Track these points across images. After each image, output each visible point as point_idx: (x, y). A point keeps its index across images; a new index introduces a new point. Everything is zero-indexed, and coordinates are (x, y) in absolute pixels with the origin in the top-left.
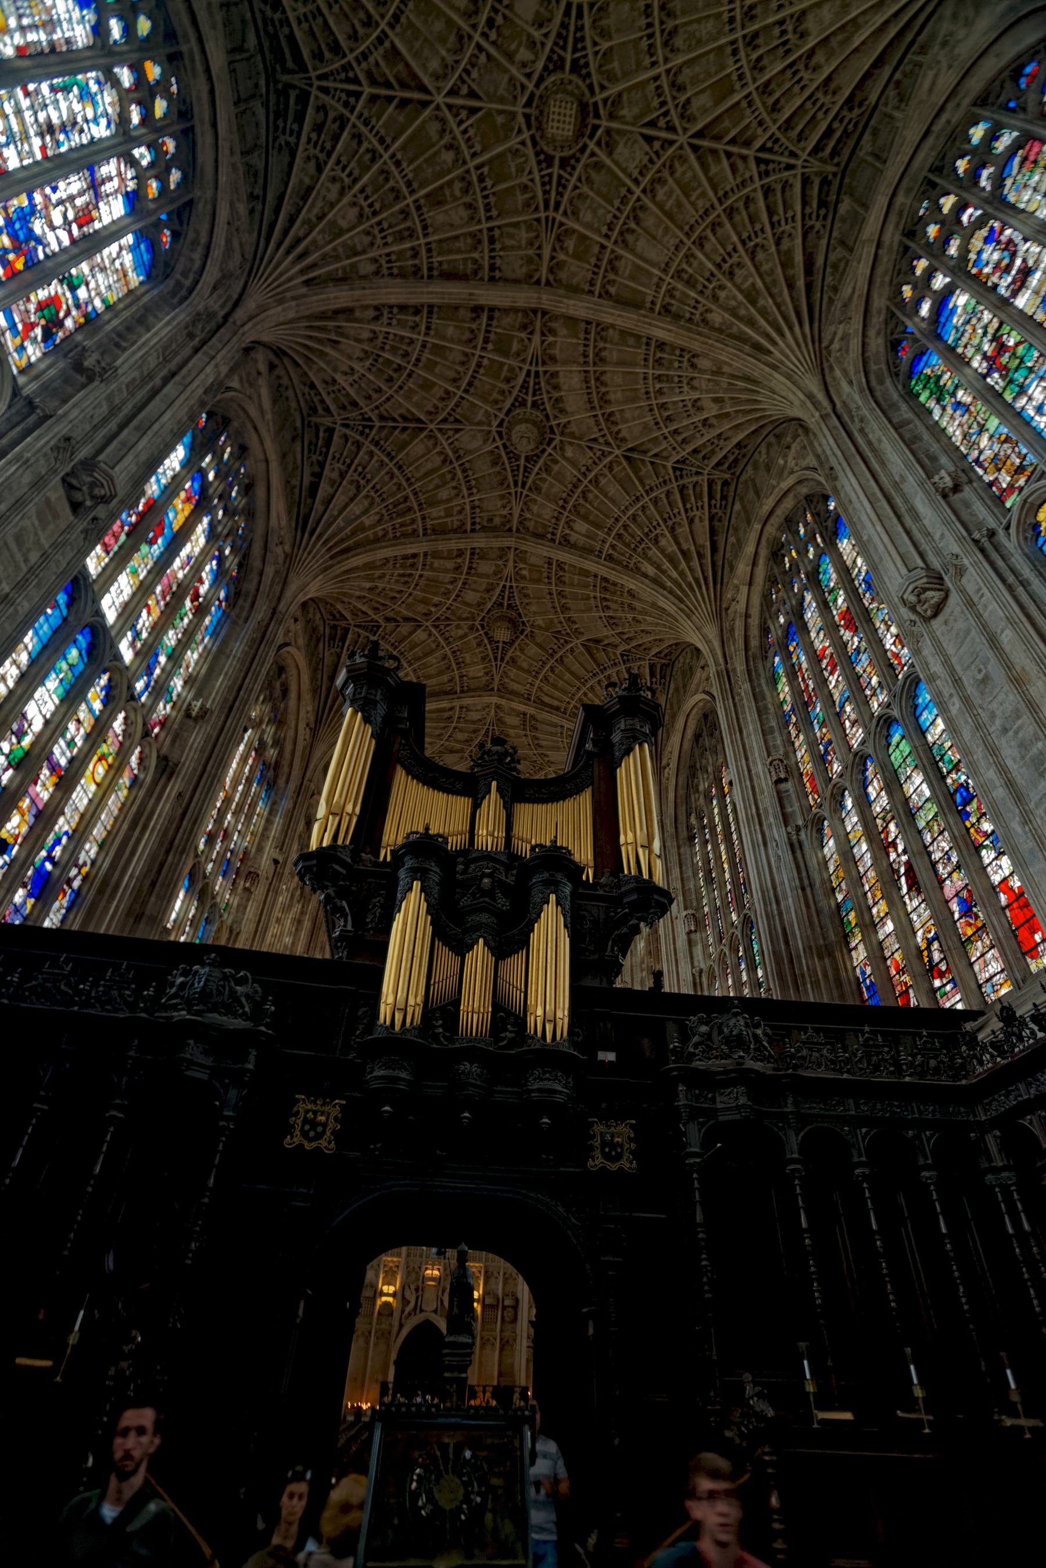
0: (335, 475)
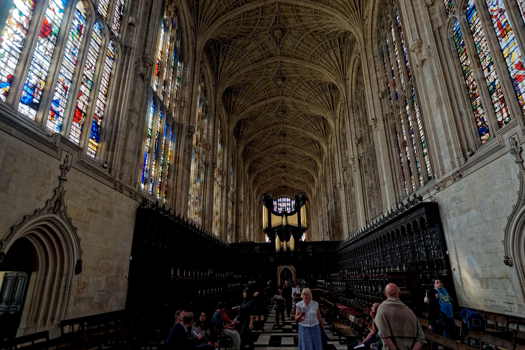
0: (243, 127)
